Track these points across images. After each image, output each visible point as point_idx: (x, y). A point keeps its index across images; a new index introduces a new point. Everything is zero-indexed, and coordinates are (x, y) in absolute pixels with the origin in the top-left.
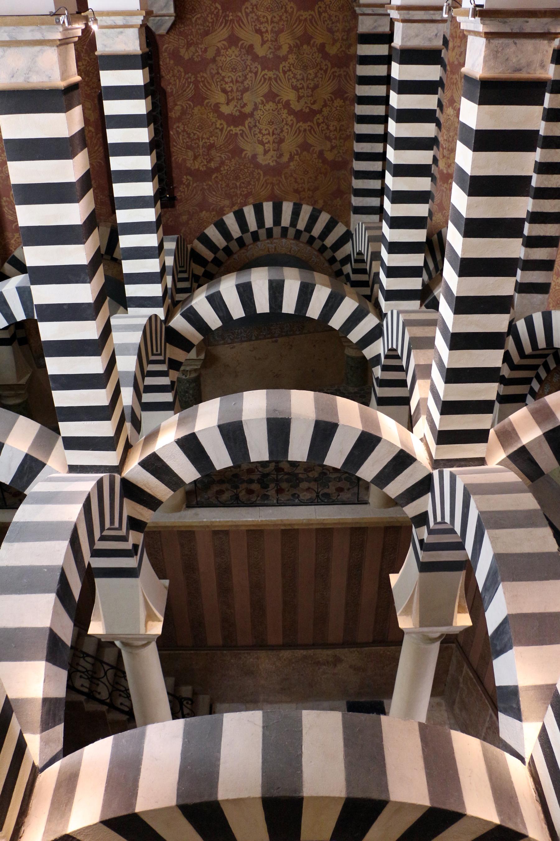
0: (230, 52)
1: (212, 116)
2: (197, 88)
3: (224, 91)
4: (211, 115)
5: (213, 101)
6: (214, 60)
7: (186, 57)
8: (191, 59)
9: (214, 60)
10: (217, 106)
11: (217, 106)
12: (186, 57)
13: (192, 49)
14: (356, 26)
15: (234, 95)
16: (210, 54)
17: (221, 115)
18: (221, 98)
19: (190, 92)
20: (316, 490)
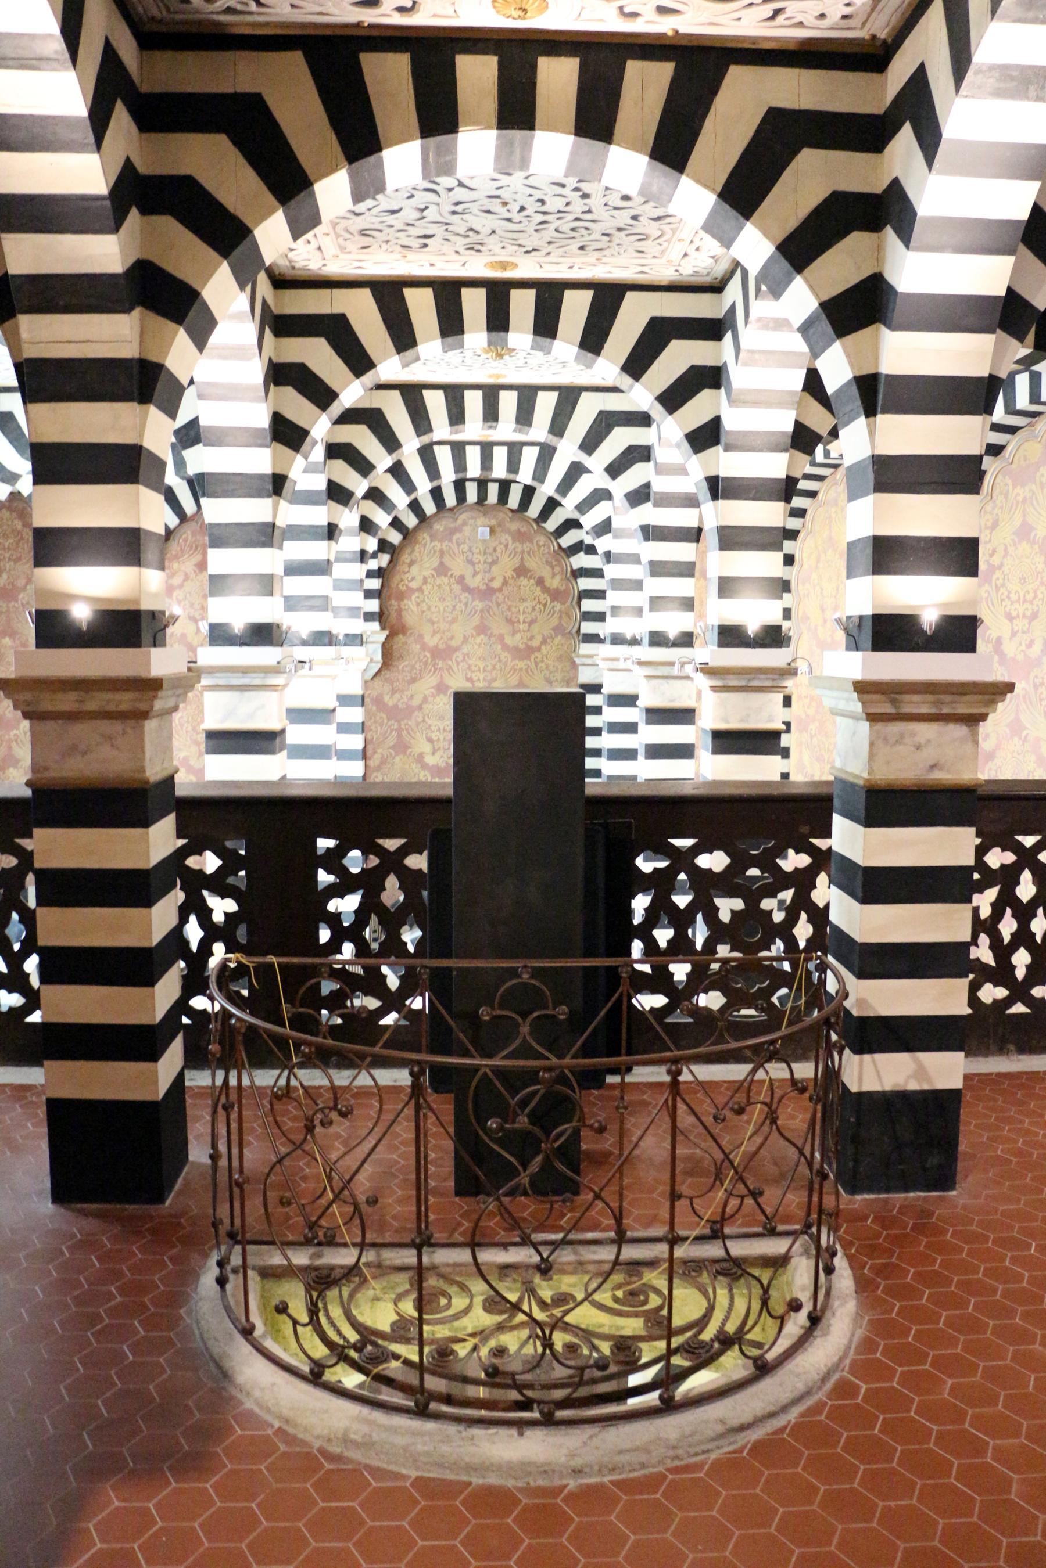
0: (438, 699)
1: (415, 767)
2: (399, 736)
3: (430, 740)
4: (414, 766)
5: (416, 751)
6: (420, 708)
7: (390, 704)
8: (396, 706)
9: (420, 708)
10: (421, 756)
11: (421, 756)
12: (390, 704)
13: (397, 696)
14: (576, 677)
15: (441, 745)
16: (415, 702)
17: (425, 766)
18: (427, 748)
19: (392, 740)
20: (548, 1351)
